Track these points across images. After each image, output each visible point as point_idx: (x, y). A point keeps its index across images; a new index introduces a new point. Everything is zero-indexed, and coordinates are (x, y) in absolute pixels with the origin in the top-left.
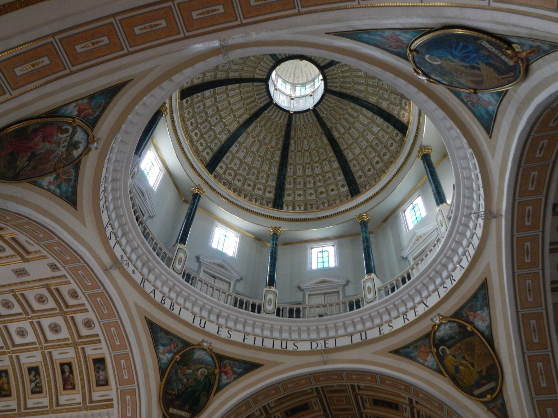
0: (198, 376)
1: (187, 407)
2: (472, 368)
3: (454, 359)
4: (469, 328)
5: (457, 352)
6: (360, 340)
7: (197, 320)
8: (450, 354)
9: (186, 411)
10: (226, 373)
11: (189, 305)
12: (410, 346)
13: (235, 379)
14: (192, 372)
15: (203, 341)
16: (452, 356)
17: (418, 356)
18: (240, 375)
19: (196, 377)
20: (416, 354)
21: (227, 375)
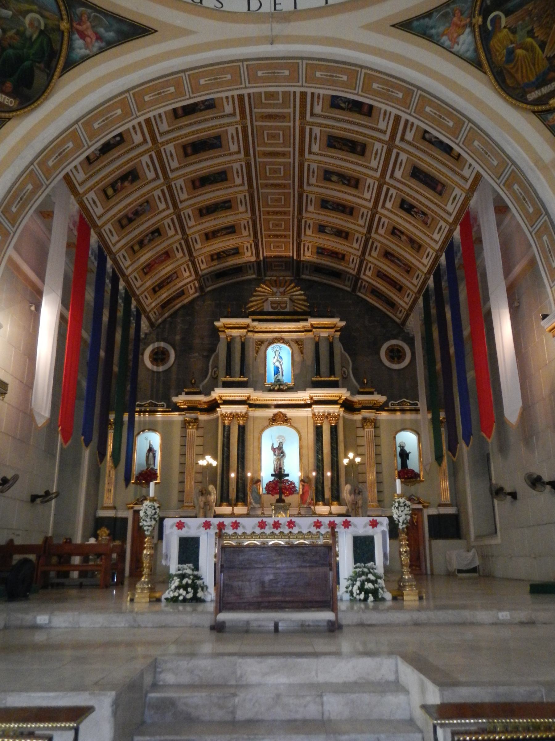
0: (25, 29)
1: (9, 85)
2: (541, 52)
3: (511, 36)
5: (520, 22)
8: (505, 27)
9: (7, 94)
10: (83, 36)
12: (435, 14)
13: (101, 50)
14: (12, 16)
16: (510, 29)
17: (443, 35)
18: (110, 44)
19: (21, 29)
20: (441, 29)
21: (84, 40)
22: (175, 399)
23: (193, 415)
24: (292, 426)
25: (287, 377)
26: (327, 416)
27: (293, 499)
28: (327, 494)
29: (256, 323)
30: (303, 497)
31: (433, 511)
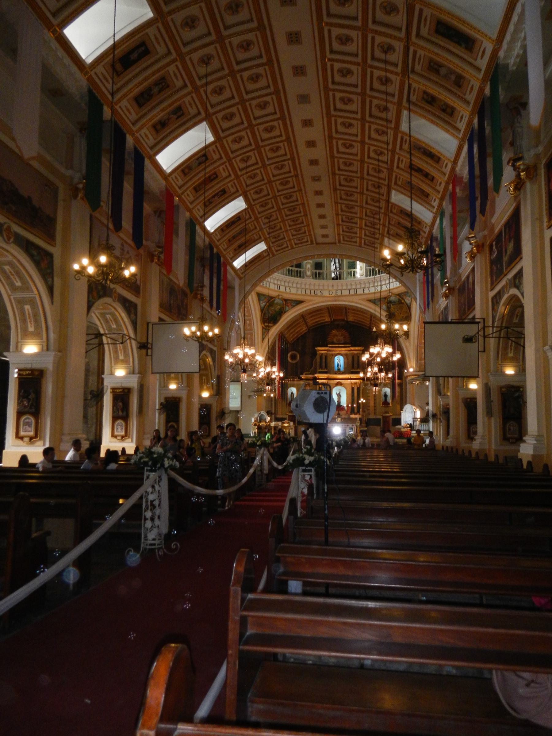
4: (403, 301)
6: (353, 293)
7: (276, 286)
11: (272, 281)
15: (279, 295)
18: (294, 306)
22: (301, 376)
23: (308, 382)
24: (344, 387)
25: (342, 368)
26: (356, 383)
27: (342, 413)
28: (356, 411)
29: (331, 349)
30: (347, 412)
31: (394, 417)
